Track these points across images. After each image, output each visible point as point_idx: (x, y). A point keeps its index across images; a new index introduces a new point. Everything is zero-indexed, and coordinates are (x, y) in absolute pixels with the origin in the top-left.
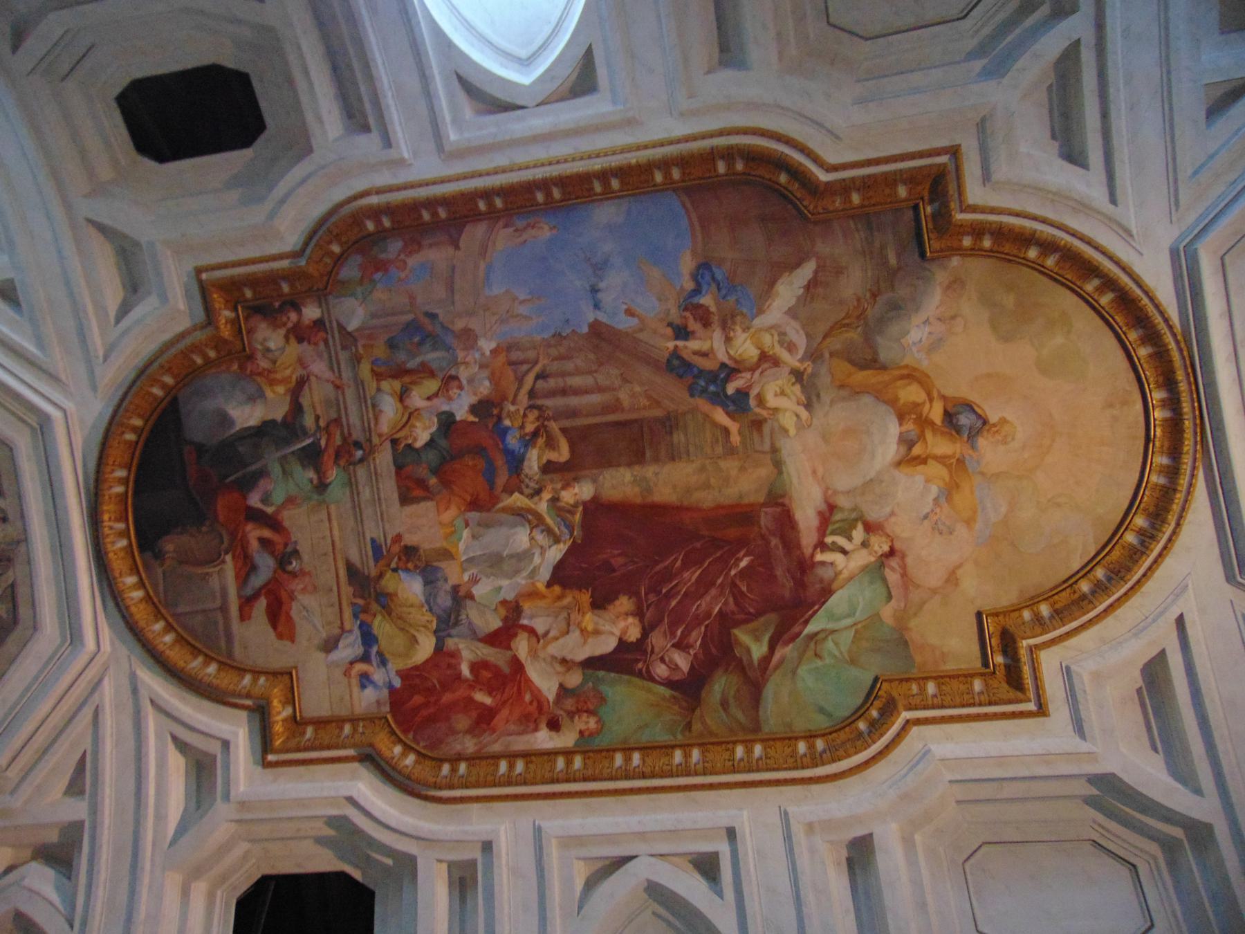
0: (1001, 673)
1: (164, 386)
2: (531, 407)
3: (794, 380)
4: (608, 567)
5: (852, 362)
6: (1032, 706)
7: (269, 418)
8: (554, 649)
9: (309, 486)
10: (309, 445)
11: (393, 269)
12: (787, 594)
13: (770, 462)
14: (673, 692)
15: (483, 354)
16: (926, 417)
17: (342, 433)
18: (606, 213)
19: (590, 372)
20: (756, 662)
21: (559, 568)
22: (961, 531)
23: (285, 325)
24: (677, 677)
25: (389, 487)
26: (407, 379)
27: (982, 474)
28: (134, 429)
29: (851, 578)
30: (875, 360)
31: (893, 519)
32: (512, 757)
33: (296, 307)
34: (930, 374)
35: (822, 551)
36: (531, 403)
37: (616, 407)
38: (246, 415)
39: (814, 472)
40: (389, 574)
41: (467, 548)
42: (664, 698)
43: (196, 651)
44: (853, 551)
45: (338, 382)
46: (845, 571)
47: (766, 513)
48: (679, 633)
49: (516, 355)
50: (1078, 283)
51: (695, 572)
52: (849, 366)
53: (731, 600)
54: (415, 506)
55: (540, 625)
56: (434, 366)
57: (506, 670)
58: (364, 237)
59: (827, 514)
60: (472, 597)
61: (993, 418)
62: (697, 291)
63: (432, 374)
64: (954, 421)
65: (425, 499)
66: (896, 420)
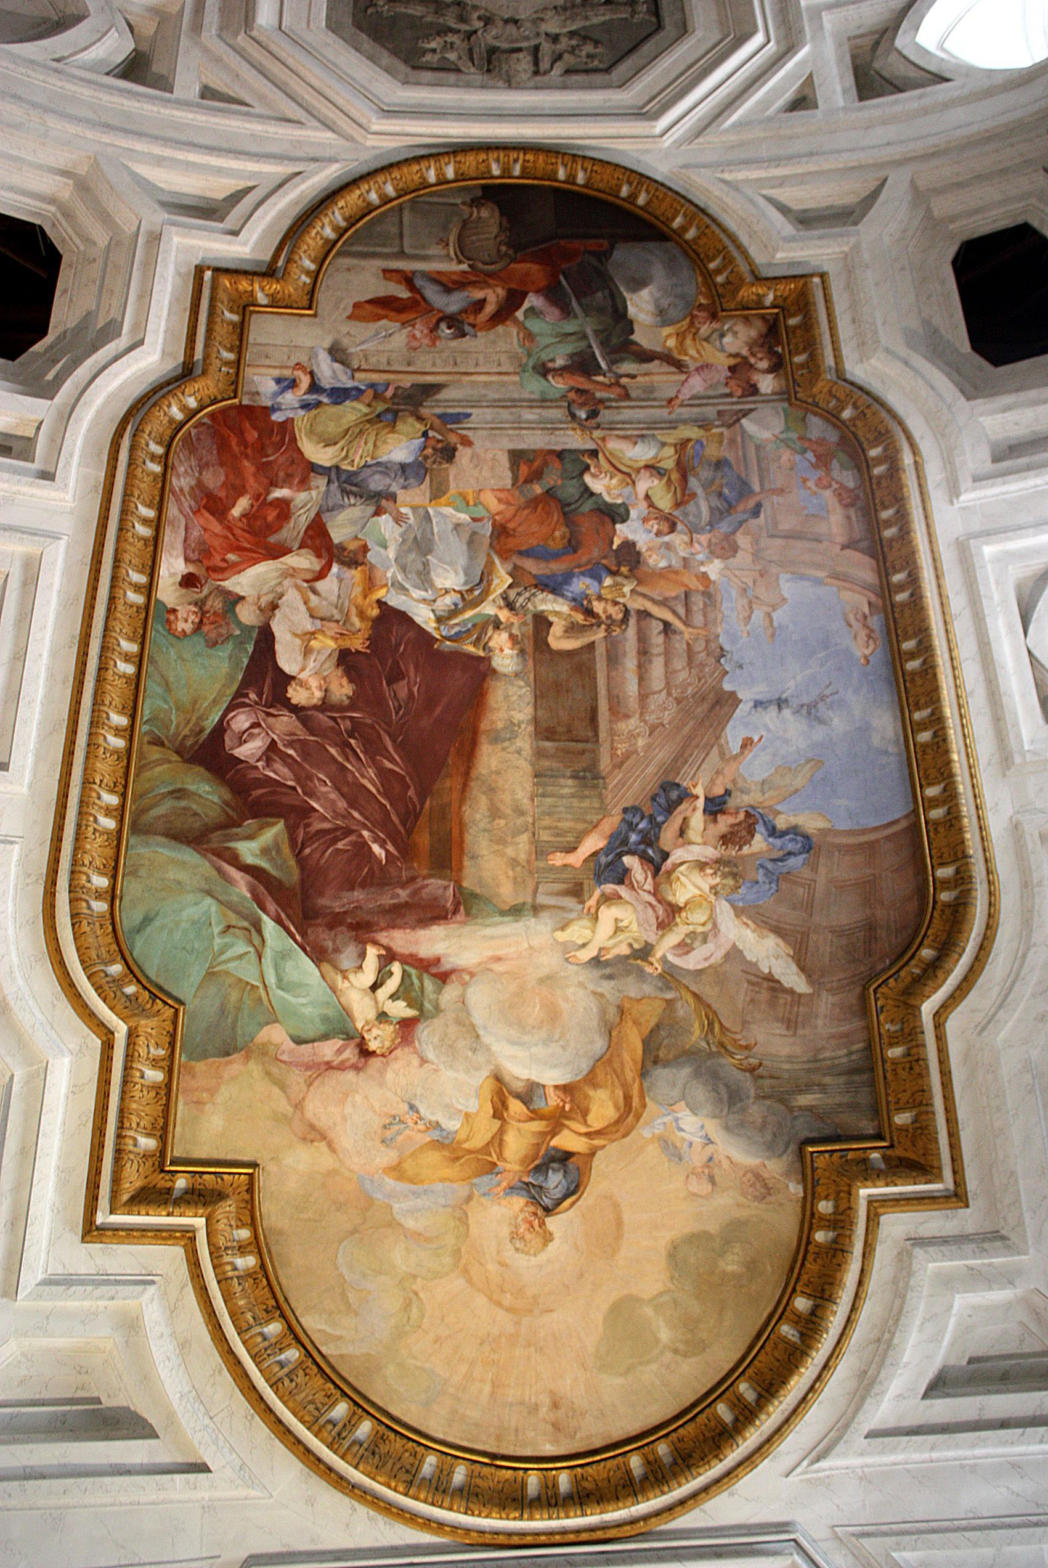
0: (161, 1181)
1: (684, 229)
2: (627, 612)
3: (636, 946)
4: (395, 676)
5: (658, 1027)
6: (100, 1218)
7: (636, 327)
8: (292, 597)
9: (544, 357)
10: (598, 364)
11: (821, 473)
12: (323, 902)
13: (521, 901)
14: (208, 731)
15: (702, 563)
16: (563, 1125)
17: (610, 400)
19: (668, 685)
20: (232, 845)
21: (403, 618)
22: (388, 1157)
23: (753, 355)
24: (228, 741)
25: (535, 441)
26: (675, 476)
27: (469, 1199)
28: (633, 197)
29: (334, 989)
30: (656, 1062)
31: (416, 1061)
32: (158, 525)
33: (776, 367)
34: (628, 1138)
35: (379, 956)
36: (632, 613)
37: (617, 711)
39: (499, 959)
40: (420, 427)
41: (444, 516)
42: (200, 718)
43: (352, 221)
44: (376, 1002)
45: (678, 402)
46: (347, 984)
47: (446, 888)
48: (291, 752)
49: (698, 602)
50: (750, 1371)
51: (375, 785)
52: (652, 1024)
53: (326, 826)
54: (507, 465)
55: (328, 586)
56: (691, 507)
57: (272, 539)
58: (861, 445)
59: (434, 970)
60: (378, 513)
61: (553, 1223)
62: (773, 832)
63: (677, 505)
64: (555, 1165)
65: (515, 479)
66: (561, 1082)
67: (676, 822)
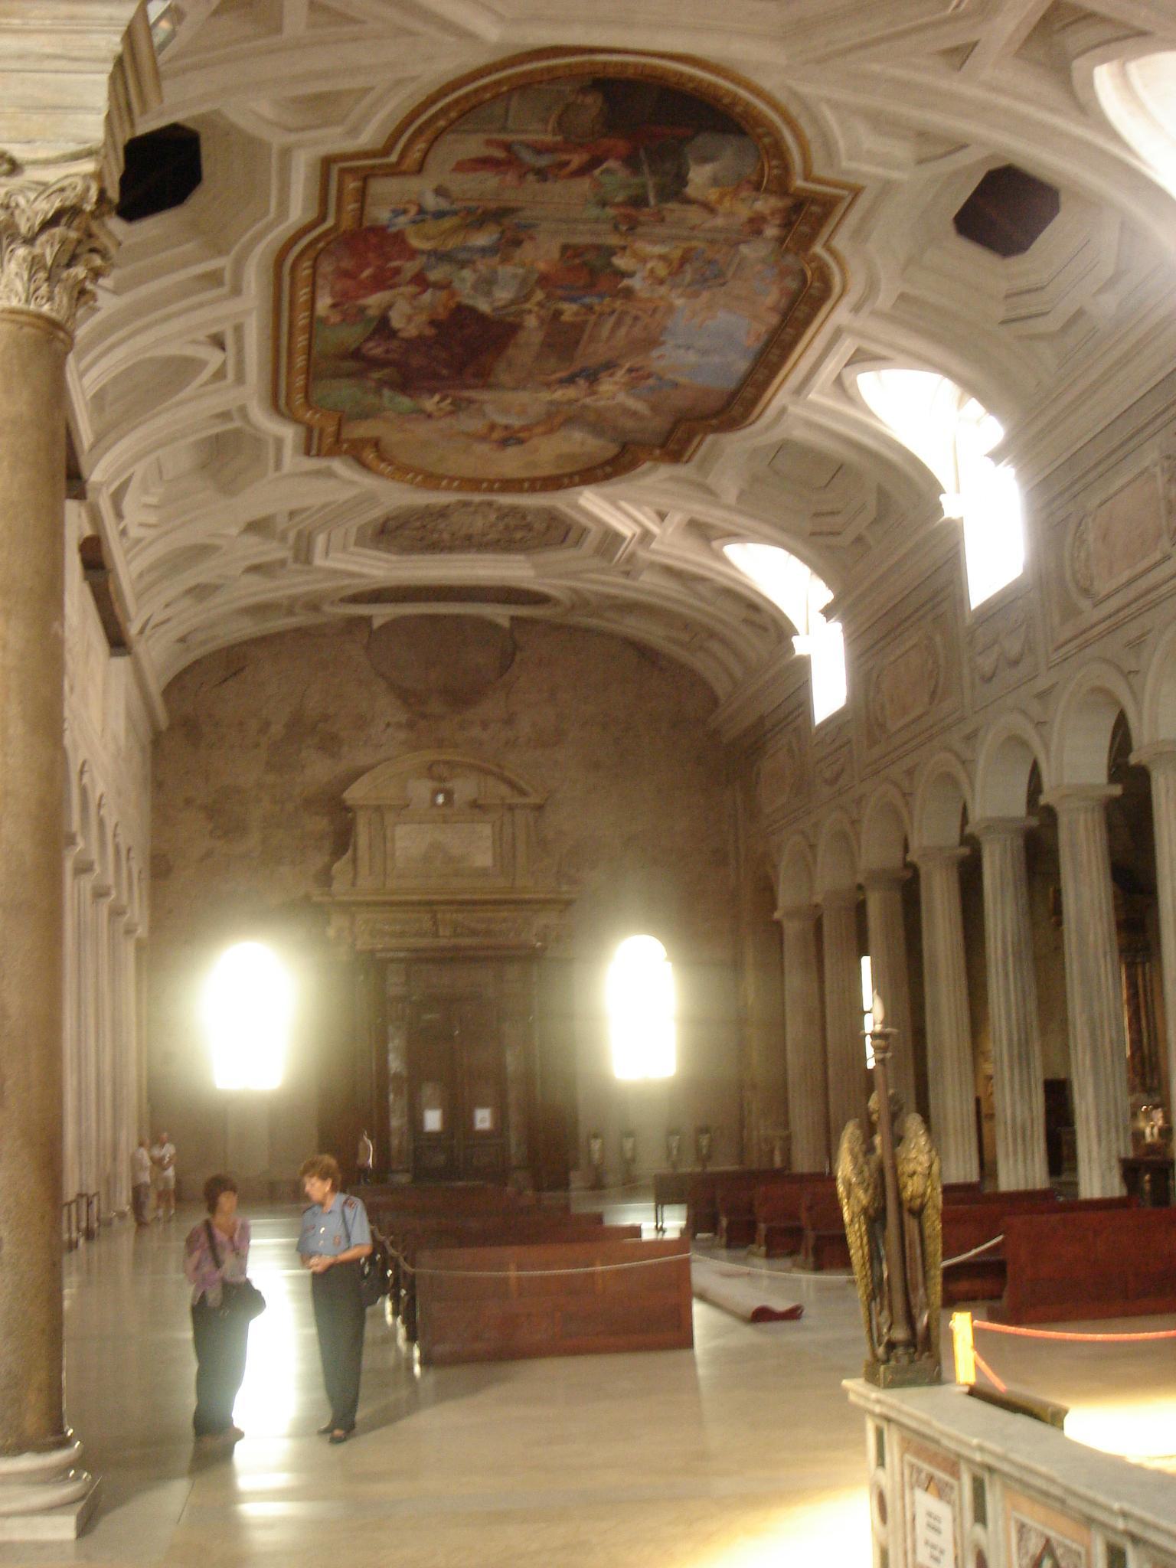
18: (742, 366)
21: (472, 310)
24: (364, 351)
26: (676, 264)
38: (699, 176)
40: (500, 229)
55: (427, 297)
57: (390, 282)
60: (462, 268)
63: (670, 274)
67: (611, 371)
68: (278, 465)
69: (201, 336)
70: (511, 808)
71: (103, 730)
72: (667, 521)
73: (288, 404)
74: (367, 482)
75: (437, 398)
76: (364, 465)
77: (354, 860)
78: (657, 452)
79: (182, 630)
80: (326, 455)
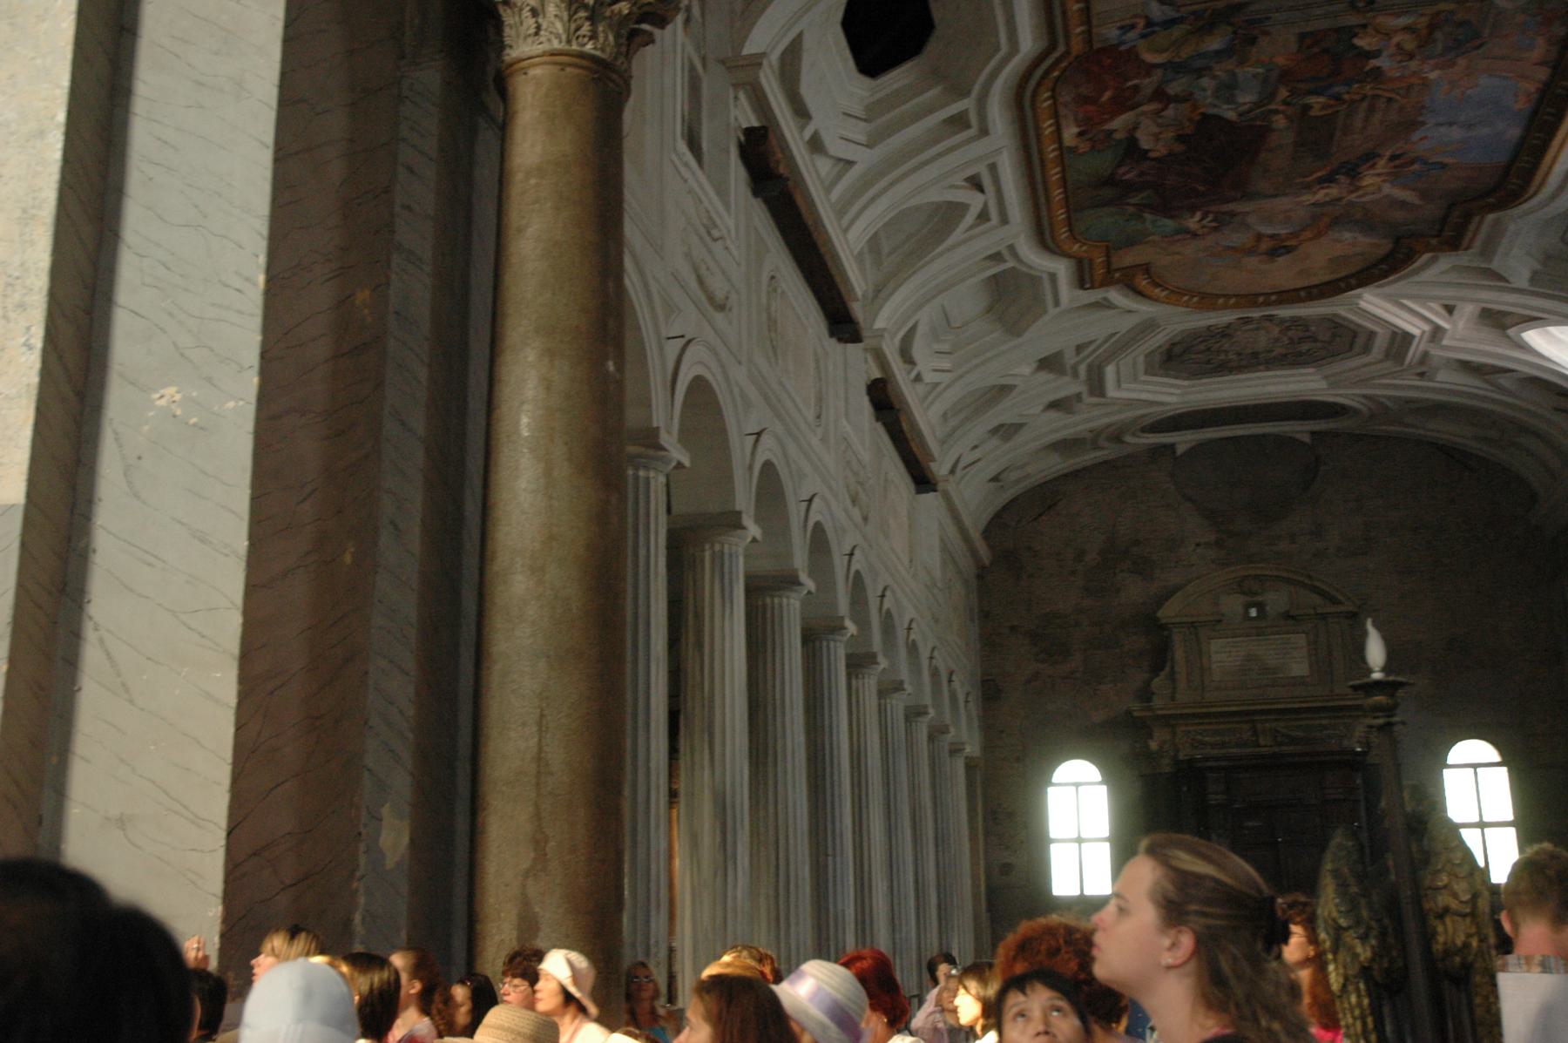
15: (1426, 73)
18: (1514, 133)
21: (1218, 118)
40: (1230, 29)
55: (1170, 112)
60: (1200, 76)
63: (1420, 47)
67: (1371, 163)
68: (1057, 303)
69: (958, 179)
70: (1323, 617)
71: (911, 561)
72: (1456, 312)
73: (1053, 238)
74: (1146, 309)
75: (1198, 215)
76: (1140, 293)
77: (1172, 677)
78: (1434, 241)
79: (992, 470)
80: (1102, 285)
